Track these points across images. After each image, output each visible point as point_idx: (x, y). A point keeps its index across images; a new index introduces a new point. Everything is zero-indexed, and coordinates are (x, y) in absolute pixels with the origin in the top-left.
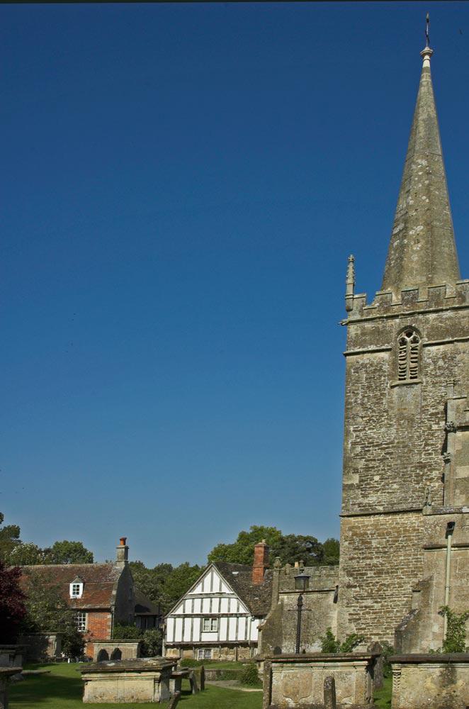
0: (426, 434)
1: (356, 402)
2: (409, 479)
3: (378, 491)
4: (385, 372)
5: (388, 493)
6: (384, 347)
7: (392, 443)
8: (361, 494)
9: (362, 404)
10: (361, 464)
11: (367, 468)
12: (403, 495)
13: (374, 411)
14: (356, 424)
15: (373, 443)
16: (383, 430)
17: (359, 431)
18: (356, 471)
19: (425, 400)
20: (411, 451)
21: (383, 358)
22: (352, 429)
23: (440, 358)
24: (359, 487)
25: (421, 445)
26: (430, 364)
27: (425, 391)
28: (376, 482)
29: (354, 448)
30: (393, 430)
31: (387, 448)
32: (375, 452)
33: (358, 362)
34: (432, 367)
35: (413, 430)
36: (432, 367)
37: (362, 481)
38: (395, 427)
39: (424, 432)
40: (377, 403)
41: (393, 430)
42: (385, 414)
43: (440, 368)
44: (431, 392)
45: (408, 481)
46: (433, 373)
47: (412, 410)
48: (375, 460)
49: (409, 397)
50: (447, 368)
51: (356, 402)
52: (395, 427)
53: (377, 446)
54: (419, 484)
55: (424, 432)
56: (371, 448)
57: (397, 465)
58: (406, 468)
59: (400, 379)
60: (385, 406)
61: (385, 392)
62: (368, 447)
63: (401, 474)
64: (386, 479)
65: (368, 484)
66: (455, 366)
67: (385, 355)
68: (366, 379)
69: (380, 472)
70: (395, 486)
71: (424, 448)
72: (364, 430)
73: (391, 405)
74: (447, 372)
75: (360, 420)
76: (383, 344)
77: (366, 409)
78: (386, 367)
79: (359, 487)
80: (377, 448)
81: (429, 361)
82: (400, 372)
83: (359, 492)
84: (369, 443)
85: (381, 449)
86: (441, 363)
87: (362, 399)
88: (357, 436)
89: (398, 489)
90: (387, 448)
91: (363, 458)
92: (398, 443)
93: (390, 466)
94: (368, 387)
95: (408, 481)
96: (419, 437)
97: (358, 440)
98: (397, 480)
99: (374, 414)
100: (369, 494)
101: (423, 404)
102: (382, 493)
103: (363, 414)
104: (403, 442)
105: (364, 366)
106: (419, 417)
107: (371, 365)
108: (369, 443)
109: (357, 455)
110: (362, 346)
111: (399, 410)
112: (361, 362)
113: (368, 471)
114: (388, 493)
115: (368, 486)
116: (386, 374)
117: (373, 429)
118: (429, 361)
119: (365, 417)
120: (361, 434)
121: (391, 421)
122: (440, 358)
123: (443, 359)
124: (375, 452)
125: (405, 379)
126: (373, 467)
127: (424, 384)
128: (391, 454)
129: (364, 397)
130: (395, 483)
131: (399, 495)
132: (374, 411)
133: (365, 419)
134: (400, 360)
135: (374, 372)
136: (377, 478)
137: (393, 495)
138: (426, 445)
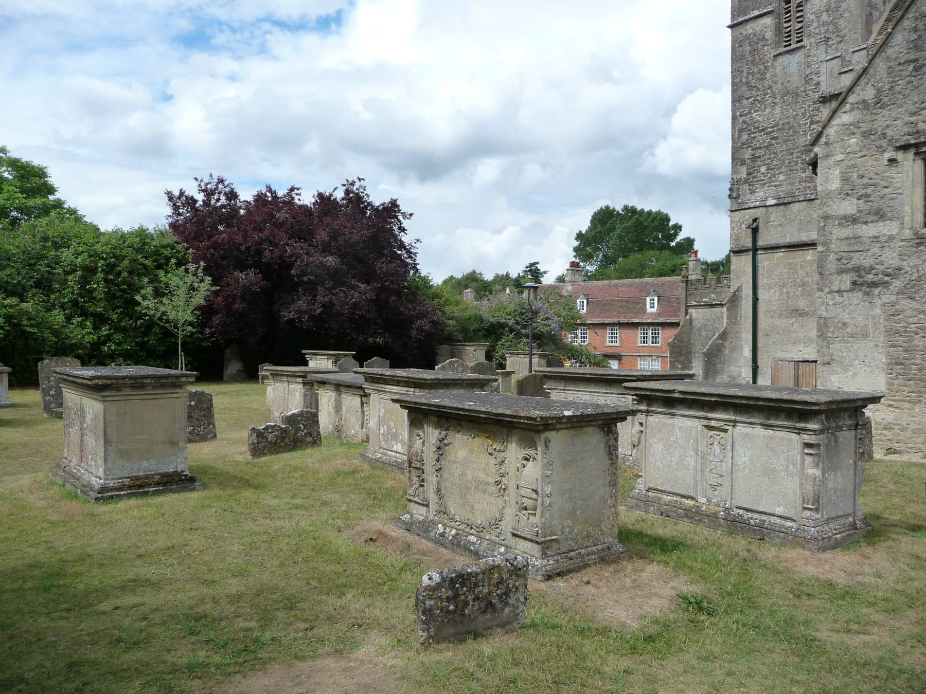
0: (811, 109)
1: (741, 81)
2: (795, 168)
3: (764, 184)
4: (768, 40)
5: (775, 186)
6: (765, 10)
7: (776, 125)
8: (749, 190)
9: (747, 83)
10: (747, 154)
11: (754, 158)
12: (789, 187)
13: (758, 90)
14: (742, 108)
15: (759, 128)
16: (768, 110)
17: (746, 115)
18: (743, 163)
19: (809, 66)
20: (795, 132)
21: (765, 23)
22: (738, 114)
23: (823, 11)
24: (746, 181)
25: (806, 124)
26: (812, 21)
27: (809, 56)
28: (762, 174)
29: (740, 136)
30: (778, 110)
31: (772, 132)
32: (762, 138)
33: (741, 34)
34: (815, 25)
35: (798, 107)
36: (815, 25)
37: (749, 174)
38: (780, 105)
39: (809, 106)
40: (762, 79)
41: (778, 110)
42: (769, 91)
43: (824, 24)
44: (815, 56)
45: (794, 170)
46: (816, 32)
47: (796, 81)
48: (760, 148)
49: (794, 69)
50: (831, 22)
51: (741, 81)
52: (780, 105)
53: (763, 130)
54: (805, 172)
55: (809, 106)
56: (757, 135)
57: (782, 151)
58: (792, 154)
59: (786, 46)
60: (767, 83)
61: (769, 64)
62: (754, 133)
63: (787, 161)
64: (772, 169)
65: (755, 177)
66: (839, 18)
67: (768, 21)
68: (750, 52)
69: (766, 162)
70: (782, 177)
71: (810, 127)
72: (750, 113)
73: (775, 79)
74: (831, 27)
75: (745, 102)
76: (765, 7)
77: (750, 88)
78: (769, 35)
79: (746, 181)
80: (762, 133)
81: (813, 17)
82: (786, 37)
83: (746, 187)
84: (755, 129)
85: (766, 134)
86: (825, 17)
87: (747, 77)
88: (744, 121)
89: (784, 181)
90: (772, 132)
91: (749, 147)
92: (783, 124)
93: (776, 153)
94: (752, 62)
95: (794, 170)
96: (804, 114)
97: (745, 126)
98: (783, 169)
99: (759, 93)
100: (757, 188)
101: (807, 73)
102: (769, 186)
103: (748, 94)
104: (788, 123)
105: (747, 37)
106: (802, 89)
107: (755, 35)
108: (755, 128)
109: (743, 144)
110: (745, 15)
111: (782, 84)
112: (745, 33)
113: (754, 162)
114: (775, 186)
115: (755, 180)
116: (769, 42)
117: (757, 111)
118: (813, 17)
119: (751, 97)
120: (747, 119)
121: (776, 98)
122: (823, 11)
123: (827, 11)
124: (762, 138)
125: (790, 45)
126: (758, 157)
127: (808, 47)
128: (776, 138)
129: (748, 74)
130: (781, 173)
131: (785, 188)
132: (758, 90)
133: (750, 100)
134: (786, 22)
135: (758, 43)
136: (763, 169)
137: (780, 189)
138: (812, 123)
